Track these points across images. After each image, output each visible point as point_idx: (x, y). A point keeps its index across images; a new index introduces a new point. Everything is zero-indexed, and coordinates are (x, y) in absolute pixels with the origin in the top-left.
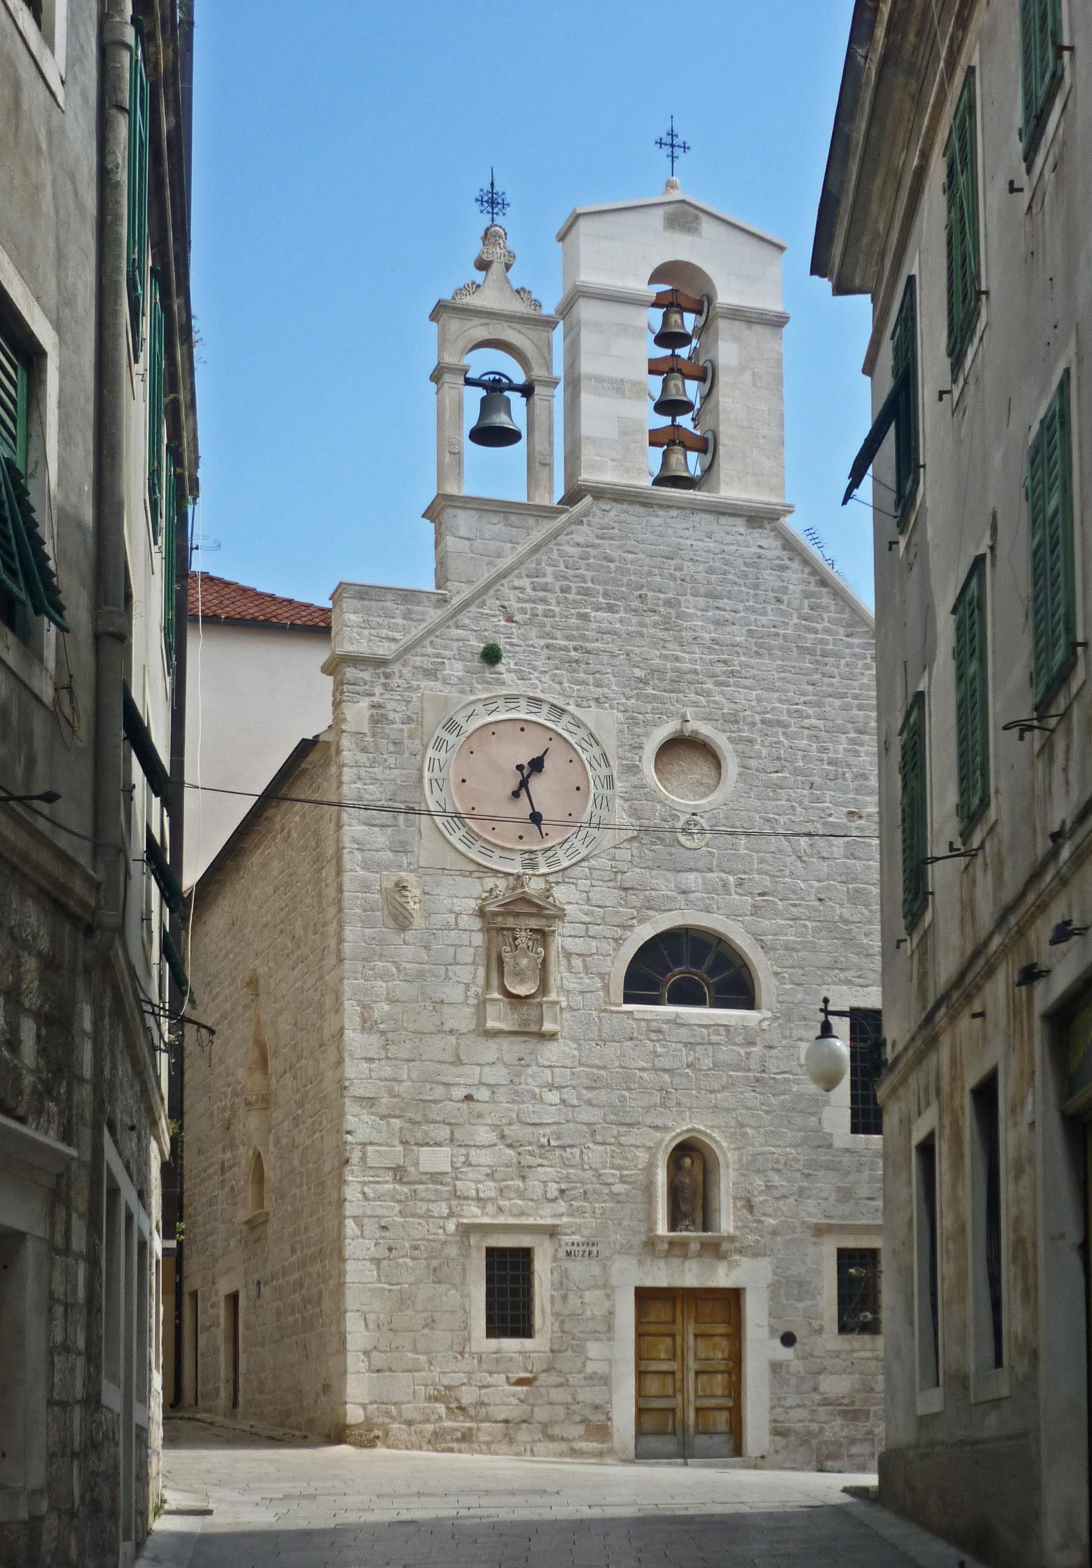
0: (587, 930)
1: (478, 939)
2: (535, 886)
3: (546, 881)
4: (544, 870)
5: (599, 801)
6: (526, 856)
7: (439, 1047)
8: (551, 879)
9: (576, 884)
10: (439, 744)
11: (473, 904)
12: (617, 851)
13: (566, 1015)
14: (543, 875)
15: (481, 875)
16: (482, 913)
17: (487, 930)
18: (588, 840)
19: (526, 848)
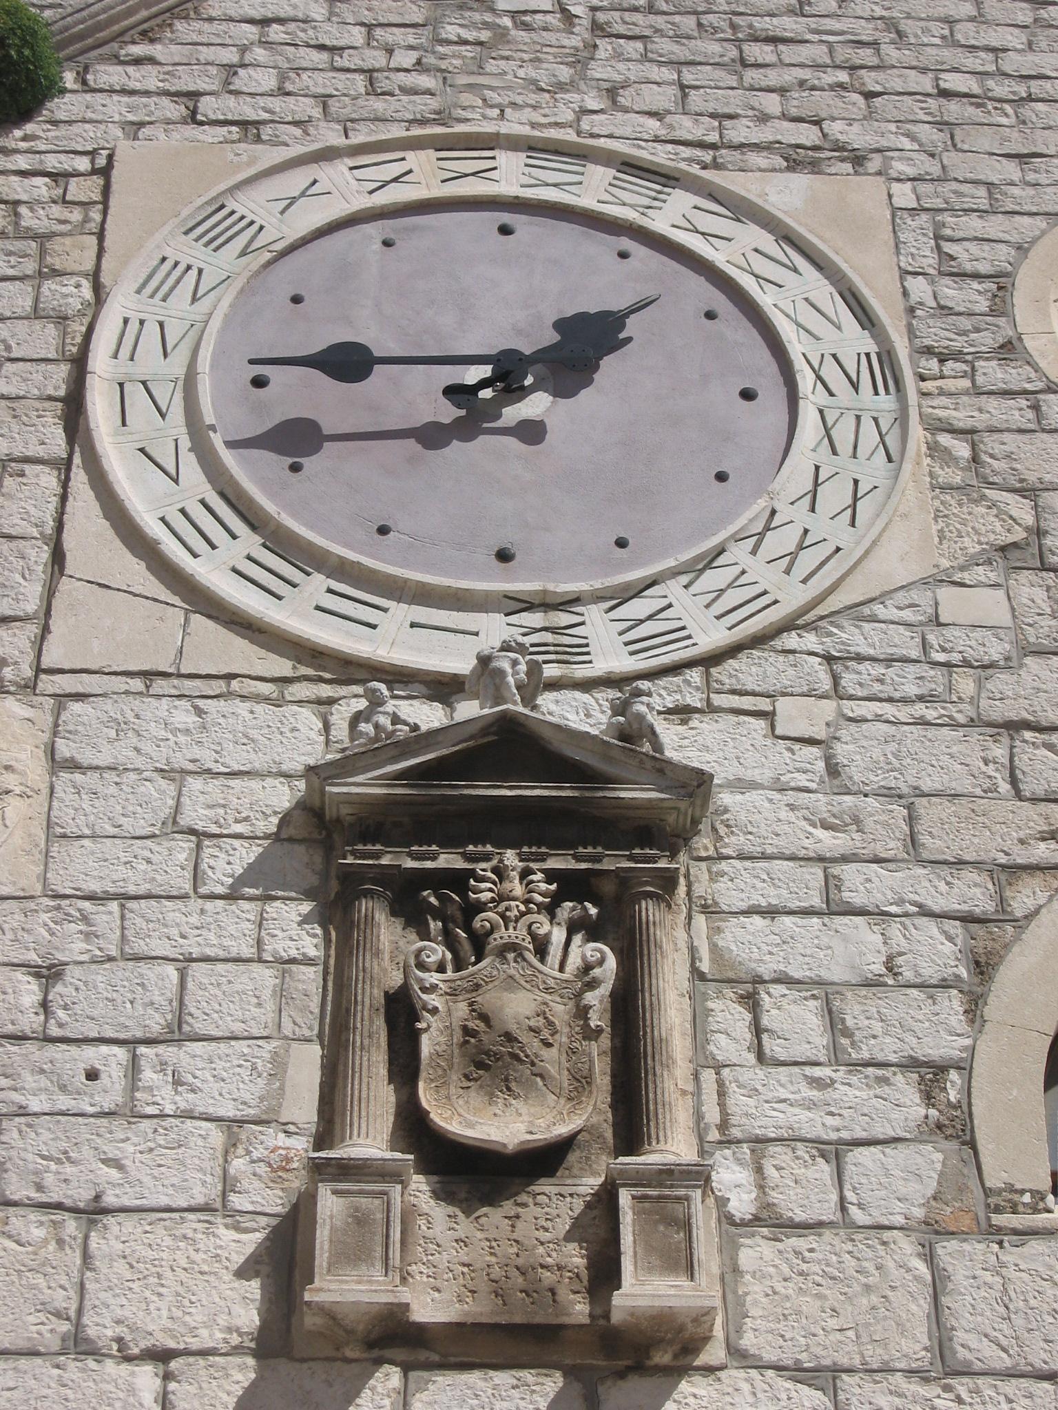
0: (831, 884)
5: (844, 434)
9: (768, 716)
10: (164, 278)
12: (944, 593)
13: (756, 1253)
15: (326, 691)
18: (808, 561)
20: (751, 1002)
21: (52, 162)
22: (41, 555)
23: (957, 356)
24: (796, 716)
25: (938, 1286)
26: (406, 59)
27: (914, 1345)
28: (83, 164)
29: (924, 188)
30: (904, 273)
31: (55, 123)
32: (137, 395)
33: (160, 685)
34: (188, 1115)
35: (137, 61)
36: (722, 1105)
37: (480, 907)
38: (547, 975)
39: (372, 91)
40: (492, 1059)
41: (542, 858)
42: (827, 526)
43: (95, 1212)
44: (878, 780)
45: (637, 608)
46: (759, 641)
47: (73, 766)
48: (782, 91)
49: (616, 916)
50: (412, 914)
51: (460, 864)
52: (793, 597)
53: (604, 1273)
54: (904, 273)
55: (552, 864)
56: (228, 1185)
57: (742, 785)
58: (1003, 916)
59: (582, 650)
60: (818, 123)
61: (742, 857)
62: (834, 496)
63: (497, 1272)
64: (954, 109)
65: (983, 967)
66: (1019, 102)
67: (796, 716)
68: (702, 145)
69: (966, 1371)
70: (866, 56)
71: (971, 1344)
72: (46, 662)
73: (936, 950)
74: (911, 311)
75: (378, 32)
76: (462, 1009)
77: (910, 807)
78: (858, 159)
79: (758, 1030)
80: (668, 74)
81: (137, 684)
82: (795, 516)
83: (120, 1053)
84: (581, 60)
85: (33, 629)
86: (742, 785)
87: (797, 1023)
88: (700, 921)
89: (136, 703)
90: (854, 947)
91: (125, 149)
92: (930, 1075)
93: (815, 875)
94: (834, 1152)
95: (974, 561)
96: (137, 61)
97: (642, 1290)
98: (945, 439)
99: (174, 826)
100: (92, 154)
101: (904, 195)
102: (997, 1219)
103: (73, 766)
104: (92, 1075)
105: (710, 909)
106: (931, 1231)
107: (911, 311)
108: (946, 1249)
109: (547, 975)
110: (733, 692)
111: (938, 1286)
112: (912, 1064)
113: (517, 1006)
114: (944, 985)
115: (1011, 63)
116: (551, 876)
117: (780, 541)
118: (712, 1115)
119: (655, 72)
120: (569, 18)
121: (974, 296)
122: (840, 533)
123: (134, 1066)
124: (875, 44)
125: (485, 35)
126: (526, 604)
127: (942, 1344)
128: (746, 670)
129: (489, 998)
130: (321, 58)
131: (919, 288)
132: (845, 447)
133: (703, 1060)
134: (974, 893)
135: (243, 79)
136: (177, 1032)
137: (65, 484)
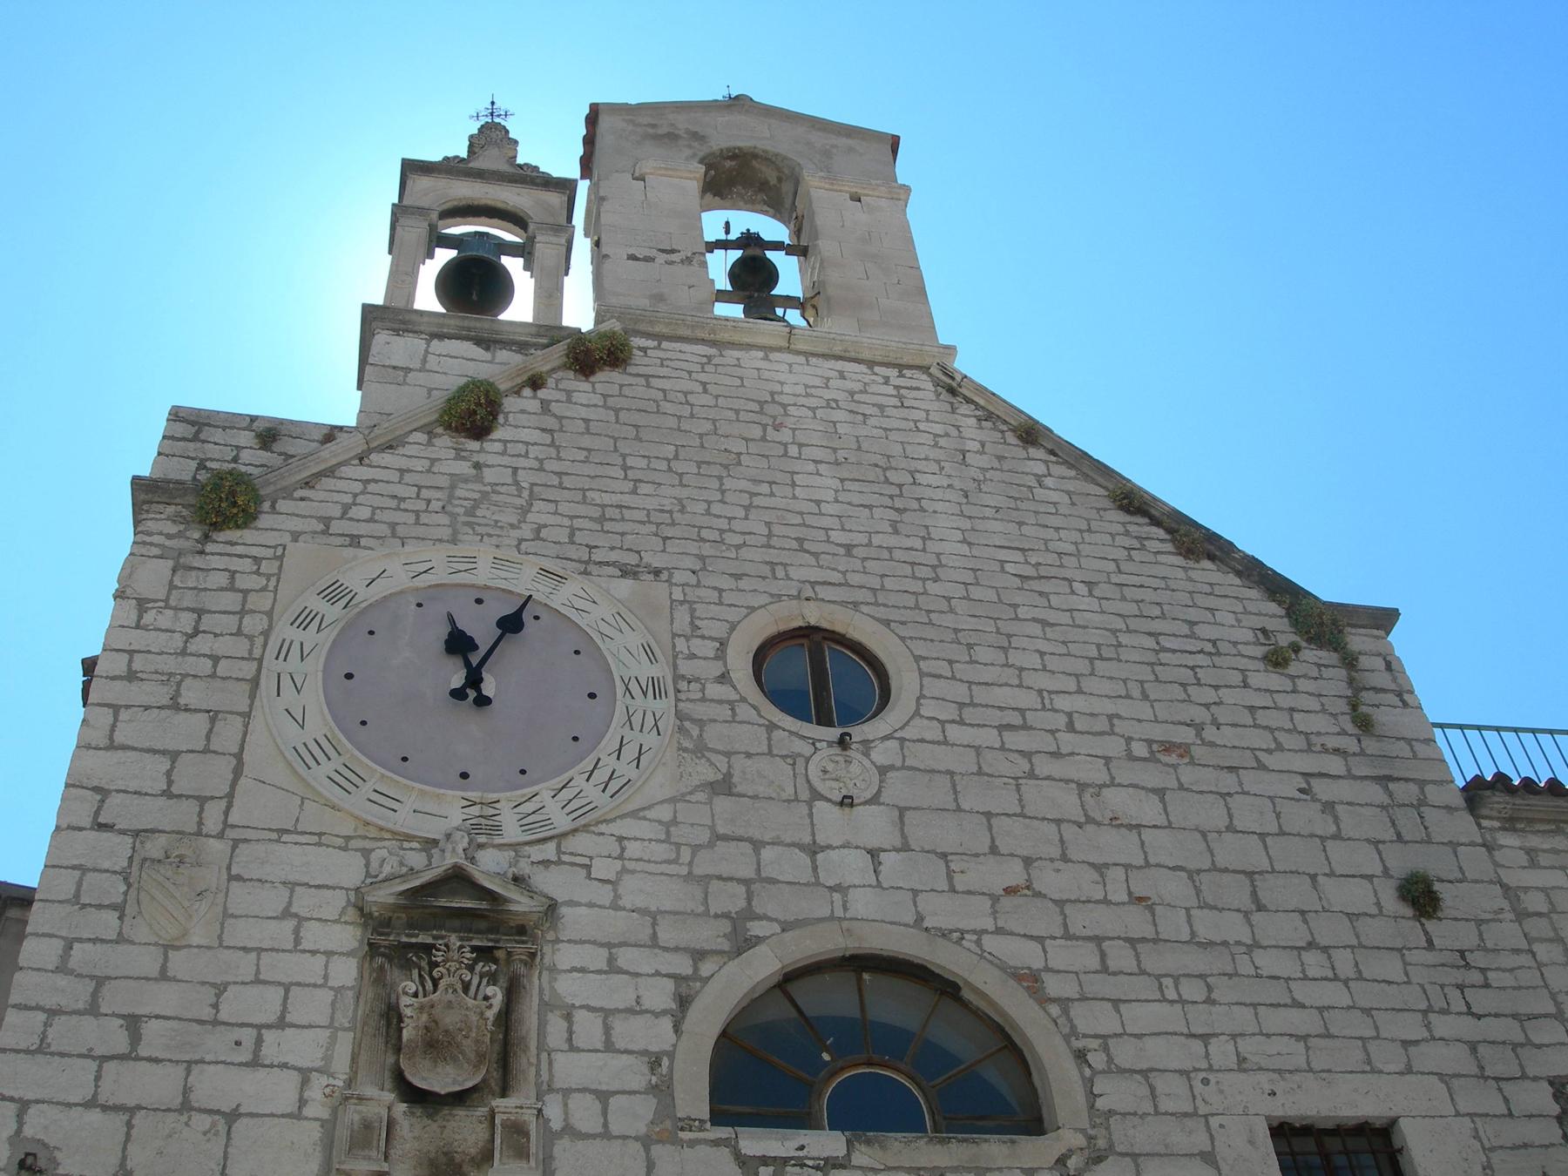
0: (611, 960)
1: (346, 972)
2: (489, 866)
5: (637, 720)
6: (475, 810)
10: (304, 620)
11: (338, 900)
15: (368, 844)
19: (474, 795)
21: (255, 551)
23: (697, 680)
24: (602, 869)
26: (436, 505)
28: (269, 553)
29: (687, 589)
30: (674, 635)
32: (286, 682)
33: (285, 838)
34: (284, 1066)
35: (302, 499)
36: (550, 1070)
37: (437, 965)
39: (417, 523)
40: (436, 1045)
41: (470, 939)
42: (626, 770)
43: (233, 1116)
44: (640, 902)
45: (529, 807)
46: (585, 828)
47: (239, 878)
48: (623, 534)
51: (430, 941)
54: (674, 635)
55: (475, 943)
56: (302, 1102)
57: (572, 903)
58: (696, 976)
59: (497, 828)
60: (638, 552)
61: (569, 941)
62: (630, 752)
63: (432, 1155)
64: (707, 550)
65: (684, 1002)
66: (738, 547)
67: (602, 869)
68: (580, 561)
70: (666, 517)
72: (230, 820)
73: (660, 995)
74: (675, 657)
75: (424, 491)
76: (424, 1017)
77: (654, 919)
79: (570, 1032)
80: (566, 522)
81: (274, 836)
82: (609, 763)
83: (254, 1032)
84: (525, 511)
85: (224, 803)
86: (572, 903)
87: (588, 1028)
88: (545, 973)
89: (276, 847)
90: (619, 993)
91: (290, 546)
93: (604, 952)
96: (302, 499)
98: (687, 724)
99: (286, 914)
100: (275, 547)
101: (678, 594)
102: (682, 1135)
103: (239, 878)
104: (238, 1043)
105: (553, 969)
106: (646, 1142)
107: (675, 657)
108: (657, 1150)
110: (571, 854)
112: (645, 1053)
113: (450, 1020)
114: (664, 1012)
115: (736, 526)
116: (474, 949)
117: (601, 775)
118: (545, 1076)
119: (558, 520)
120: (520, 489)
121: (709, 648)
122: (632, 773)
123: (259, 1041)
124: (671, 512)
125: (477, 496)
129: (437, 1011)
130: (393, 504)
131: (681, 644)
132: (637, 727)
133: (541, 1047)
134: (683, 966)
135: (353, 513)
136: (281, 1024)
137: (246, 726)
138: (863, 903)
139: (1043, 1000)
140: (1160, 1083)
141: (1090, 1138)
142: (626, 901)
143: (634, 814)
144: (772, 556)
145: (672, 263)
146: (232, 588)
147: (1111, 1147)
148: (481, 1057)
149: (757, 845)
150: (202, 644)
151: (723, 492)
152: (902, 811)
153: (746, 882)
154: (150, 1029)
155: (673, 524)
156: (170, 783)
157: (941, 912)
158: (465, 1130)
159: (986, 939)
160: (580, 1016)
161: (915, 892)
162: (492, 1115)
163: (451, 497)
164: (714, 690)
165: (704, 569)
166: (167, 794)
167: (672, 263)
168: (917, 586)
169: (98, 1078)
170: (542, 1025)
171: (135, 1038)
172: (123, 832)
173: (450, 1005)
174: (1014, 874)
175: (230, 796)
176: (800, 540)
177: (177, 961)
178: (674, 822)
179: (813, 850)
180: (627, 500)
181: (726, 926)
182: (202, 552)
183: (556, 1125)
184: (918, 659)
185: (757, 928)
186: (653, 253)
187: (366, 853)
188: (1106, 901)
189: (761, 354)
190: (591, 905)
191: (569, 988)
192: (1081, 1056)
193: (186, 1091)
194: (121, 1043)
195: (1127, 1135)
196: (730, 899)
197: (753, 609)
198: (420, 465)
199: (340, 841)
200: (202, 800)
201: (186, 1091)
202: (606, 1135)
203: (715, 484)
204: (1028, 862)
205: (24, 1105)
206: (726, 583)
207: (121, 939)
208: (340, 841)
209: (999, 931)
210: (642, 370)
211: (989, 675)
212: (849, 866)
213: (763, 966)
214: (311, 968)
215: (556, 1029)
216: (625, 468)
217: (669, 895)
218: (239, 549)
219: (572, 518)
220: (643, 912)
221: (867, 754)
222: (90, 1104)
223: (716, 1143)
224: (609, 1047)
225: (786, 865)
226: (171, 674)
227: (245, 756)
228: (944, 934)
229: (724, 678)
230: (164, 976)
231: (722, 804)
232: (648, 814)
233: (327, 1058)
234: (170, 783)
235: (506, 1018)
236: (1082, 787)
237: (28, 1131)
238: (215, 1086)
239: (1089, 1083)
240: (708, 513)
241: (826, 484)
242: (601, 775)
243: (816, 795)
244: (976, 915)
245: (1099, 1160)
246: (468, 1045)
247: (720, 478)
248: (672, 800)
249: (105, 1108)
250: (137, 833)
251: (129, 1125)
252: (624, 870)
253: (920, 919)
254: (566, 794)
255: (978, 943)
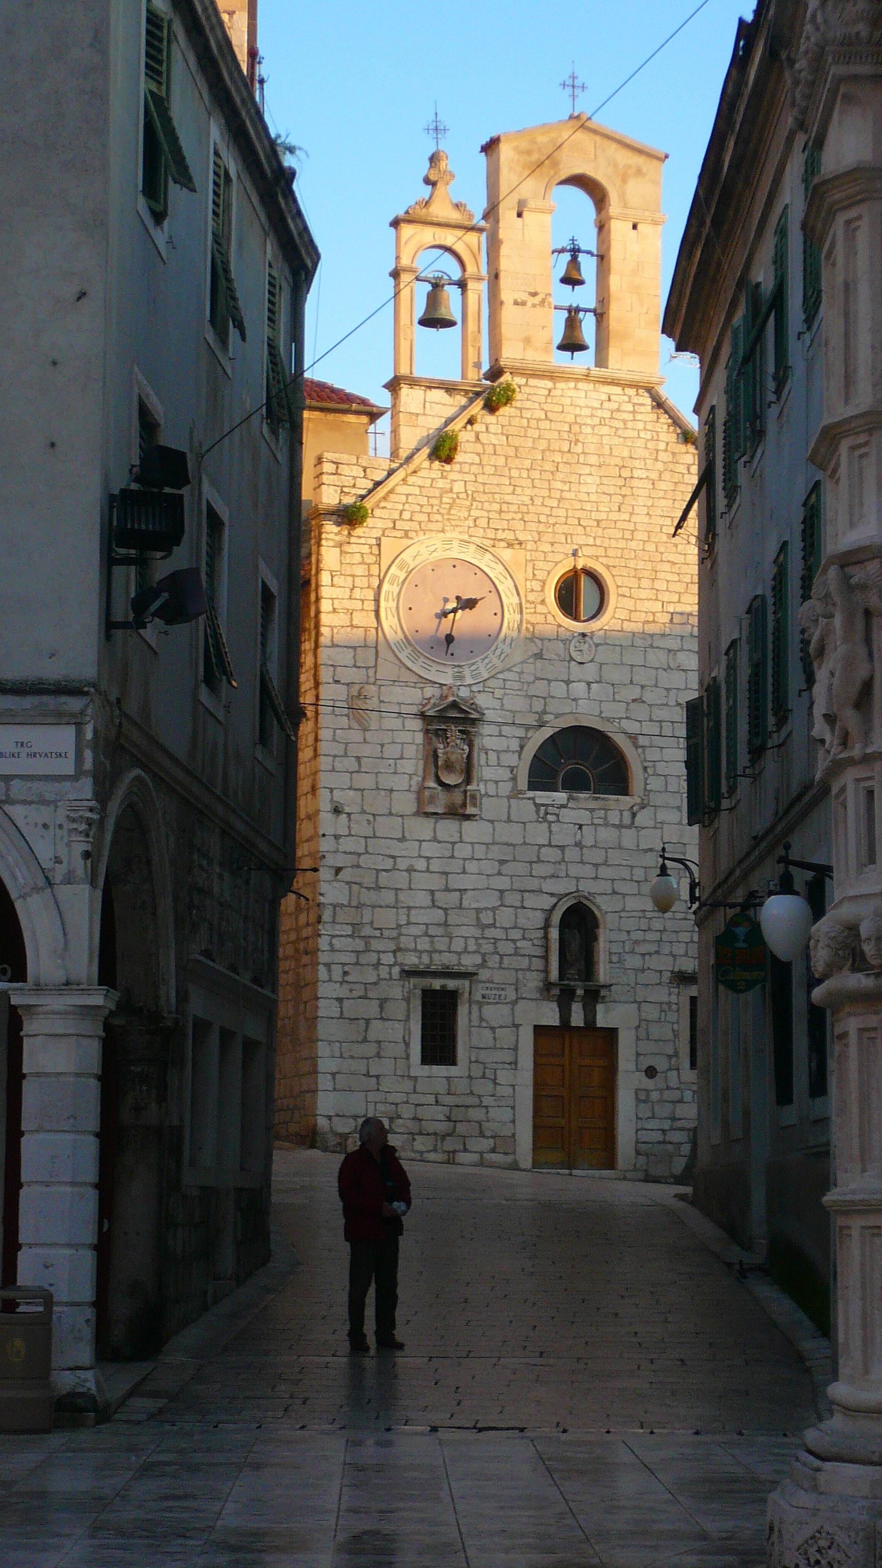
0: (500, 731)
1: (419, 738)
3: (471, 691)
4: (469, 681)
6: (456, 670)
7: (386, 827)
8: (475, 688)
12: (524, 665)
14: (470, 685)
16: (422, 715)
17: (427, 732)
18: (502, 657)
19: (456, 664)
20: (486, 753)
22: (374, 650)
25: (509, 807)
26: (435, 508)
27: (505, 818)
30: (526, 580)
31: (367, 527)
33: (396, 684)
37: (447, 738)
38: (457, 750)
40: (449, 767)
42: (507, 650)
43: (391, 791)
45: (473, 668)
49: (468, 738)
50: (437, 735)
52: (500, 666)
53: (464, 805)
56: (410, 786)
67: (498, 693)
69: (511, 822)
71: (513, 818)
73: (515, 745)
78: (520, 544)
80: (485, 514)
86: (488, 709)
87: (493, 756)
92: (512, 769)
94: (496, 782)
95: (531, 657)
96: (384, 508)
97: (470, 810)
105: (481, 735)
106: (509, 798)
109: (457, 750)
111: (509, 807)
112: (509, 766)
113: (453, 757)
117: (498, 652)
121: (537, 586)
123: (396, 764)
126: (456, 666)
127: (509, 817)
128: (491, 683)
134: (521, 732)
136: (402, 758)
138: (584, 706)
139: (637, 747)
140: (669, 779)
141: (643, 799)
142: (506, 707)
143: (509, 670)
144: (566, 529)
145: (534, 306)
146: (363, 563)
147: (648, 804)
148: (462, 771)
149: (549, 681)
150: (357, 593)
151: (550, 490)
152: (601, 664)
153: (544, 698)
154: (364, 760)
155: (528, 513)
156: (355, 661)
157: (610, 710)
158: (458, 797)
159: (623, 720)
160: (490, 753)
161: (601, 701)
162: (465, 792)
163: (441, 503)
164: (540, 608)
165: (539, 540)
166: (355, 666)
167: (534, 306)
168: (622, 544)
169: (351, 779)
170: (479, 755)
171: (360, 765)
172: (343, 684)
173: (453, 753)
174: (636, 692)
175: (376, 666)
176: (579, 519)
177: (369, 735)
178: (522, 672)
179: (568, 682)
180: (508, 498)
181: (537, 716)
182: (349, 543)
183: (483, 793)
184: (618, 587)
185: (547, 718)
186: (524, 296)
187: (422, 688)
188: (666, 705)
189: (572, 385)
190: (494, 709)
191: (488, 742)
192: (645, 768)
193: (377, 783)
194: (355, 767)
195: (655, 799)
196: (538, 706)
197: (557, 563)
198: (428, 483)
199: (413, 685)
200: (367, 668)
201: (377, 783)
202: (497, 796)
203: (546, 485)
204: (643, 687)
205: (332, 790)
206: (547, 548)
207: (350, 728)
208: (413, 685)
209: (627, 718)
210: (518, 404)
211: (643, 594)
212: (579, 689)
213: (547, 732)
214: (408, 737)
215: (483, 756)
216: (510, 478)
217: (520, 704)
218: (363, 541)
219: (488, 511)
220: (511, 711)
221: (592, 638)
222: (350, 788)
223: (529, 799)
224: (499, 765)
225: (559, 689)
226: (348, 610)
227: (379, 649)
228: (608, 719)
229: (543, 602)
230: (365, 741)
231: (539, 663)
232: (514, 669)
233: (416, 770)
234: (355, 661)
235: (469, 757)
236: (670, 651)
237: (335, 799)
238: (387, 782)
239: (646, 779)
240: (543, 505)
241: (591, 483)
242: (498, 652)
243: (572, 659)
244: (618, 710)
245: (643, 808)
246: (458, 768)
247: (549, 481)
248: (522, 662)
249: (356, 790)
250: (348, 684)
251: (363, 796)
252: (505, 694)
253: (601, 712)
254: (486, 661)
255: (619, 723)
